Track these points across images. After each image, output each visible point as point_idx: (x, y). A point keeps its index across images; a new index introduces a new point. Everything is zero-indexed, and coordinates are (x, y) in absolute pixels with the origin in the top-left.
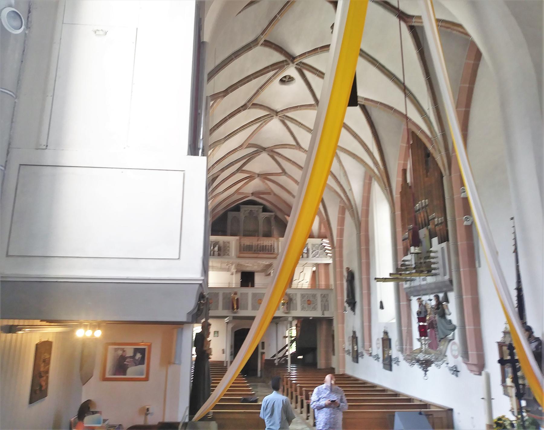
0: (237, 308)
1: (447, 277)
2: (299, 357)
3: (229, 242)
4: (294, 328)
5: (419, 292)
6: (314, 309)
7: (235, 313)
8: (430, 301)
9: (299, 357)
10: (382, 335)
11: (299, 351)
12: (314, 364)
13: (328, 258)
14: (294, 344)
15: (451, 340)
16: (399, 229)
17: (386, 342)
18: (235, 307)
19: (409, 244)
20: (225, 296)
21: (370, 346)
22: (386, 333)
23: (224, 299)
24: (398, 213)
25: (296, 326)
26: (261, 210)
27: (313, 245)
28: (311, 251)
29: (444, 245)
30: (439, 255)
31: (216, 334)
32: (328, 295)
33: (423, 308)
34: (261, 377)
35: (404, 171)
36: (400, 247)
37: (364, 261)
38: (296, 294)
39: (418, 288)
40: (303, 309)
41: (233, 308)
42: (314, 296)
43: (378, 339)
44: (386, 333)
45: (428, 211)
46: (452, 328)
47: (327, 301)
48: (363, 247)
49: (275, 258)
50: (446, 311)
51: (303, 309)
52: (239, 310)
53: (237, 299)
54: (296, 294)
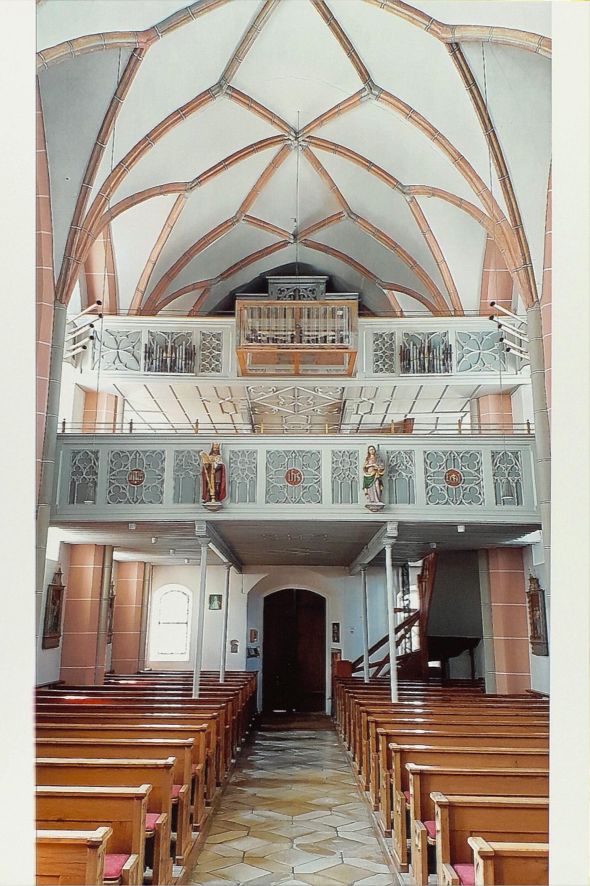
0: (220, 495)
2: (433, 664)
3: (218, 337)
4: (414, 587)
6: (475, 497)
7: (215, 510)
9: (433, 664)
11: (432, 645)
12: (474, 685)
13: (511, 370)
14: (415, 630)
18: (212, 492)
20: (183, 460)
23: (178, 467)
25: (420, 578)
26: (323, 287)
27: (464, 337)
28: (455, 354)
31: (216, 604)
32: (515, 454)
34: (333, 714)
38: (409, 453)
40: (432, 497)
41: (207, 497)
42: (472, 458)
47: (513, 471)
49: (350, 374)
51: (432, 497)
52: (227, 502)
53: (220, 469)
54: (409, 453)
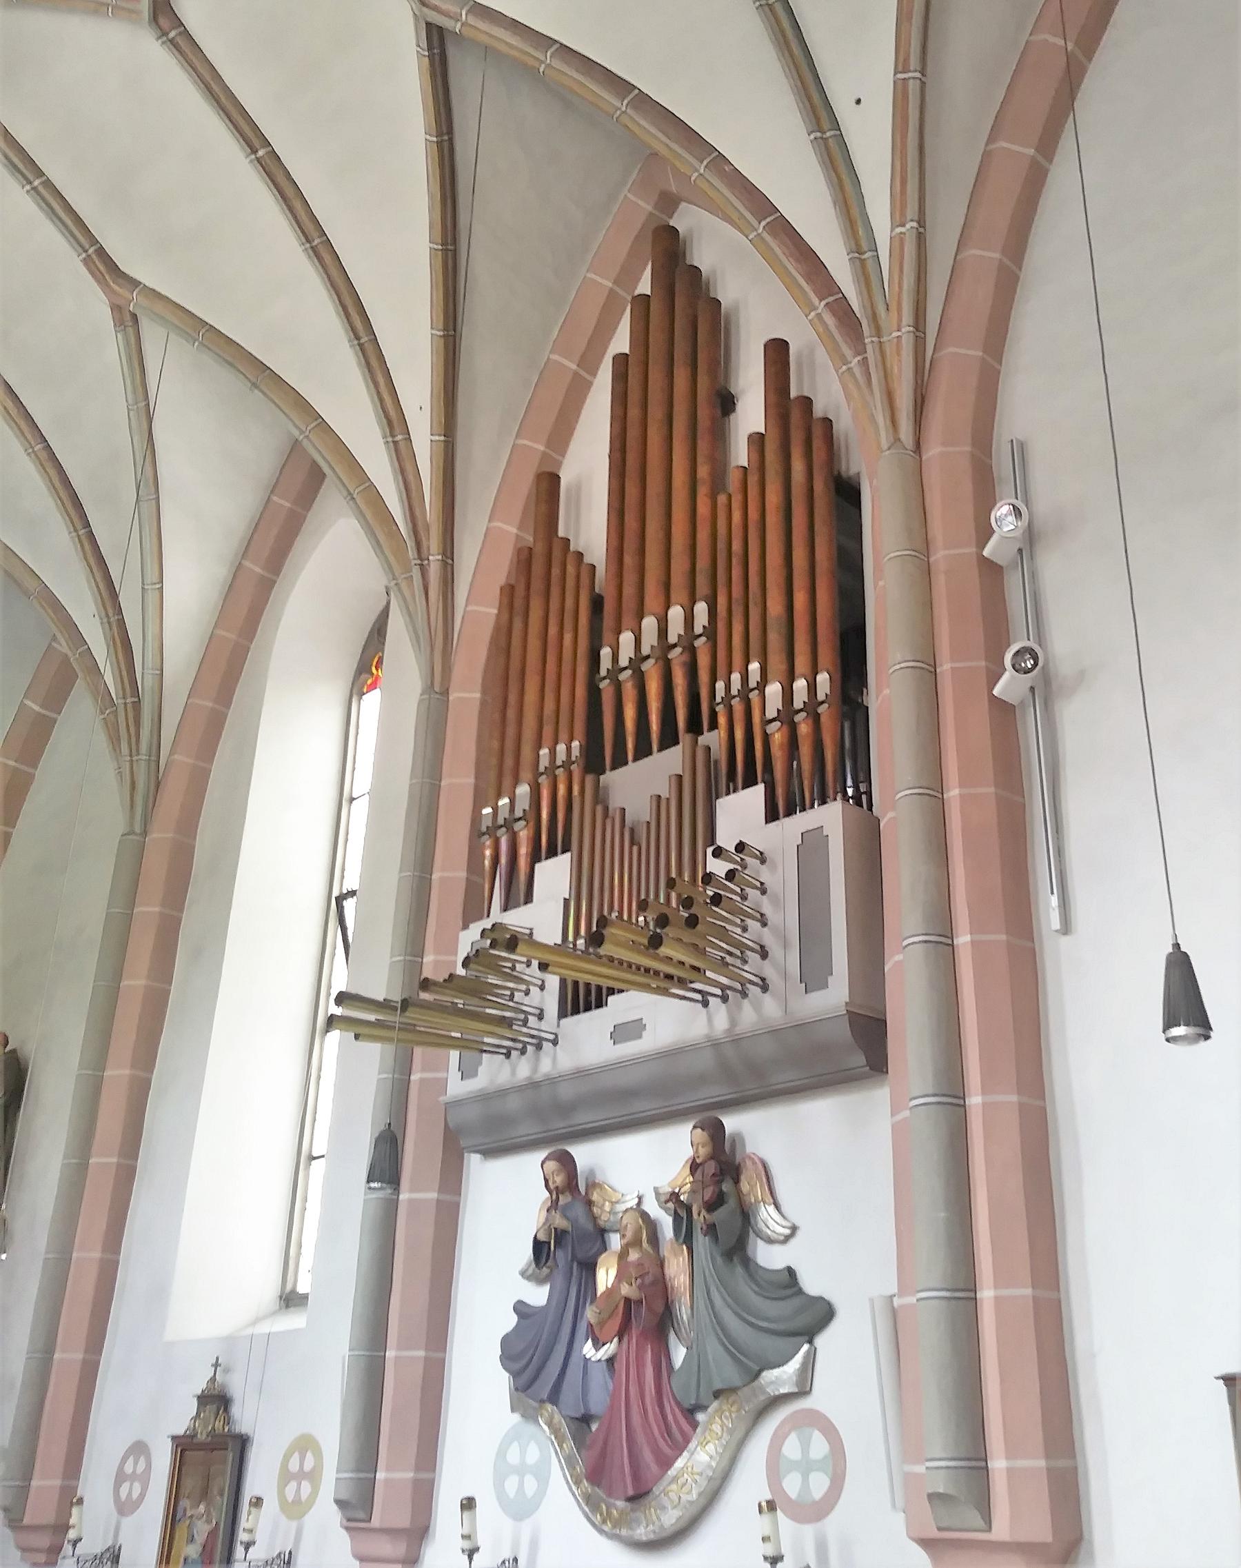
1: (836, 994)
5: (556, 1122)
8: (643, 1168)
10: (181, 1416)
15: (777, 1401)
16: (459, 779)
17: (212, 1456)
19: (523, 850)
21: (70, 1498)
22: (216, 1400)
24: (467, 695)
29: (830, 817)
30: (782, 877)
33: (579, 1211)
35: (548, 485)
36: (450, 871)
37: (135, 982)
39: (566, 1092)
43: (139, 1449)
44: (216, 1400)
45: (703, 661)
46: (800, 1322)
48: (149, 909)
50: (767, 1217)
